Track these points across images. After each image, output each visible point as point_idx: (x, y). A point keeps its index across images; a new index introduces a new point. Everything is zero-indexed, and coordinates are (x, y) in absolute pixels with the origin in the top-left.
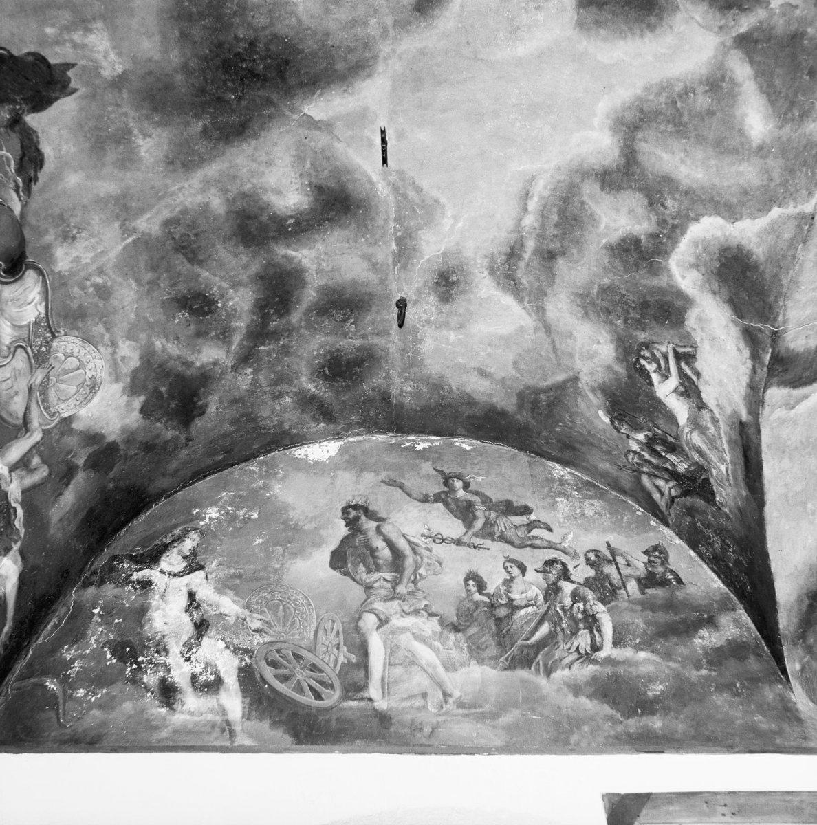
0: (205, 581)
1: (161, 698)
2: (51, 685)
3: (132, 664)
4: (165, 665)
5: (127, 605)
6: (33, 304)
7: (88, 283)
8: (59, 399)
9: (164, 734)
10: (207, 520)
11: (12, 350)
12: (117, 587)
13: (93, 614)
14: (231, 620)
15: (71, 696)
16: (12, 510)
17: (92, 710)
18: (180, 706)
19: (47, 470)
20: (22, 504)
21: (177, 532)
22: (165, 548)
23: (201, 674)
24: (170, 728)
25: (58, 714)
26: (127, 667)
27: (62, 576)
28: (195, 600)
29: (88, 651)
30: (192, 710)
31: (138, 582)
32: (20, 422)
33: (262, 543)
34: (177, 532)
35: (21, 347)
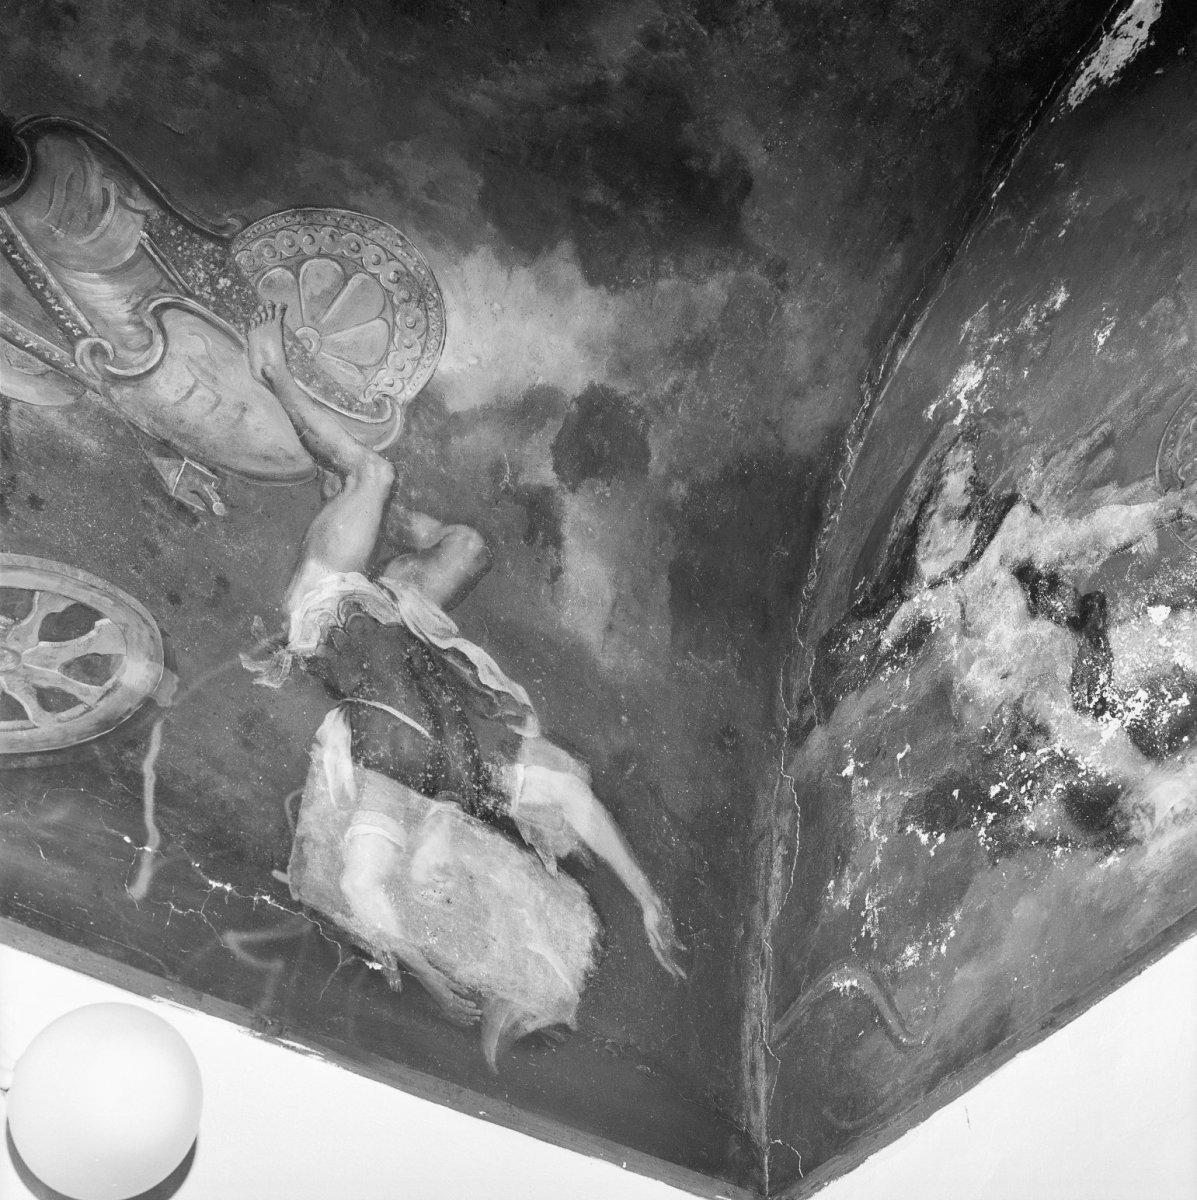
0: (1037, 519)
1: (1092, 838)
2: (845, 982)
3: (981, 816)
4: (1055, 760)
5: (904, 708)
6: (113, 203)
7: (192, 82)
8: (361, 368)
9: (1146, 911)
10: (965, 405)
11: (150, 323)
12: (863, 690)
13: (847, 781)
14: (1150, 545)
15: (894, 977)
16: (450, 659)
17: (952, 973)
18: (1146, 823)
19: (475, 535)
20: (466, 632)
21: (918, 484)
22: (913, 532)
23: (1151, 714)
24: (1152, 888)
25: (888, 1033)
26: (976, 830)
27: (721, 746)
28: (1039, 576)
29: (878, 860)
30: (1180, 809)
31: (899, 645)
32: (306, 462)
33: (1114, 332)
34: (918, 484)
35: (166, 306)
